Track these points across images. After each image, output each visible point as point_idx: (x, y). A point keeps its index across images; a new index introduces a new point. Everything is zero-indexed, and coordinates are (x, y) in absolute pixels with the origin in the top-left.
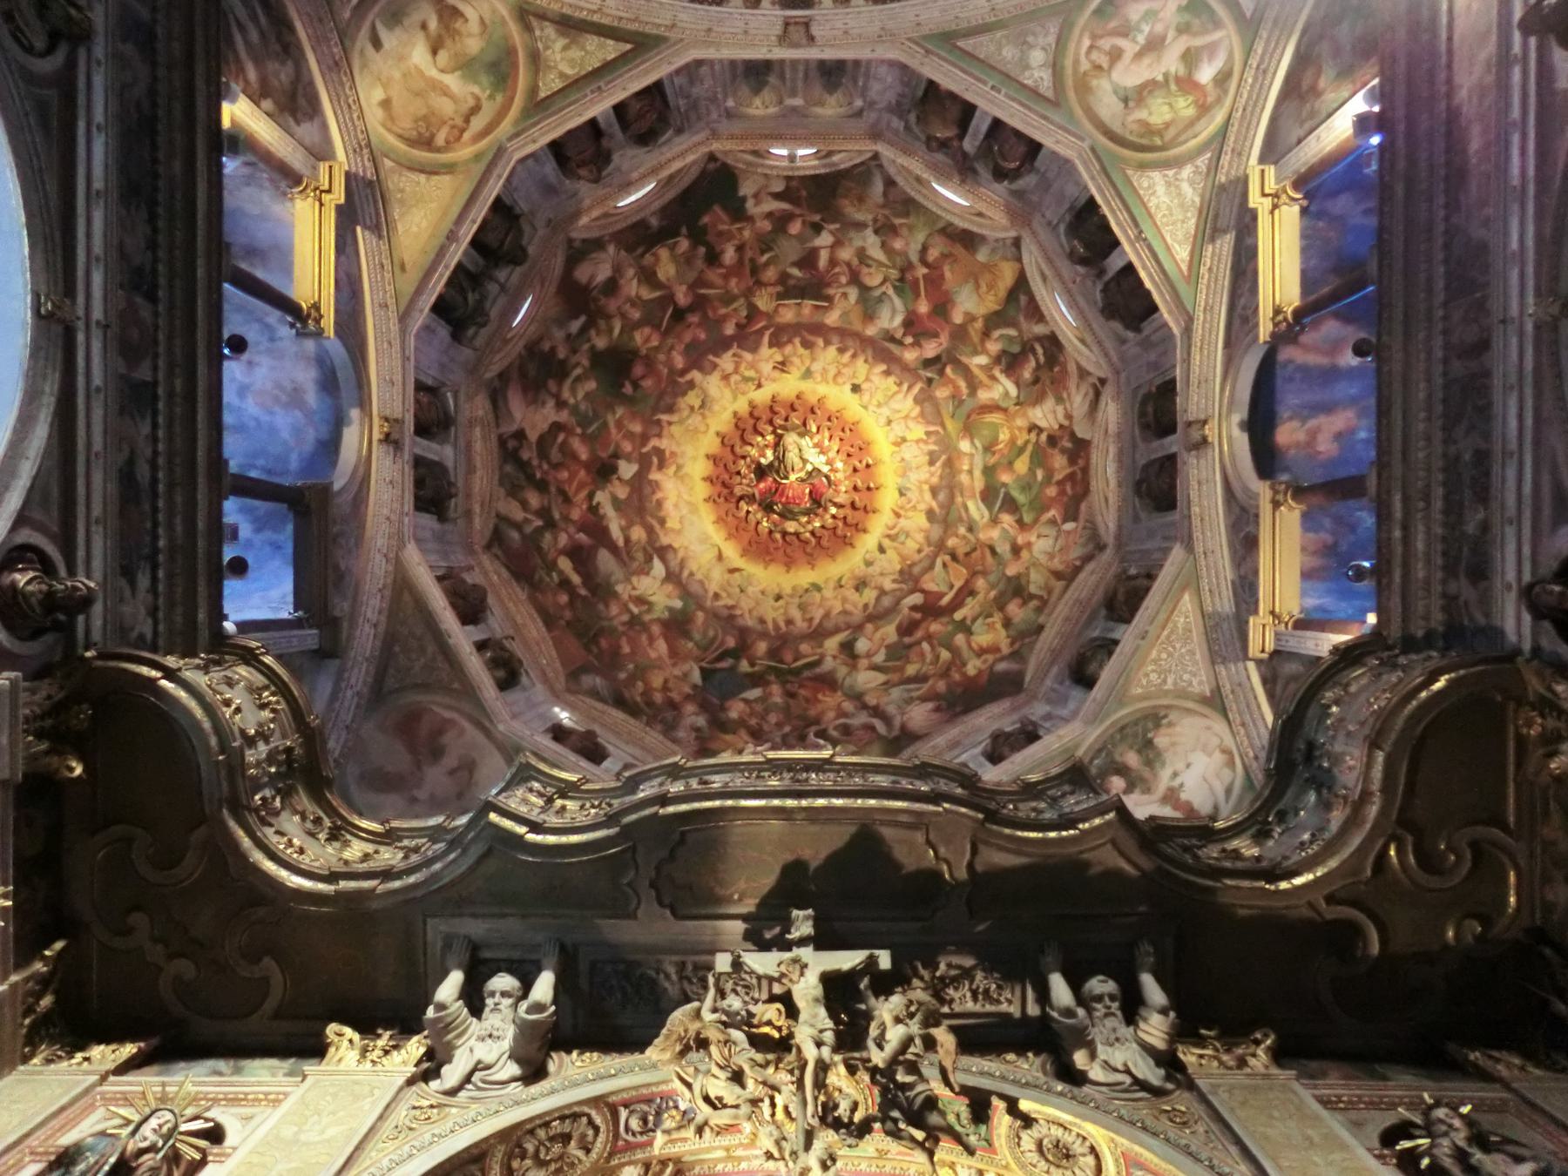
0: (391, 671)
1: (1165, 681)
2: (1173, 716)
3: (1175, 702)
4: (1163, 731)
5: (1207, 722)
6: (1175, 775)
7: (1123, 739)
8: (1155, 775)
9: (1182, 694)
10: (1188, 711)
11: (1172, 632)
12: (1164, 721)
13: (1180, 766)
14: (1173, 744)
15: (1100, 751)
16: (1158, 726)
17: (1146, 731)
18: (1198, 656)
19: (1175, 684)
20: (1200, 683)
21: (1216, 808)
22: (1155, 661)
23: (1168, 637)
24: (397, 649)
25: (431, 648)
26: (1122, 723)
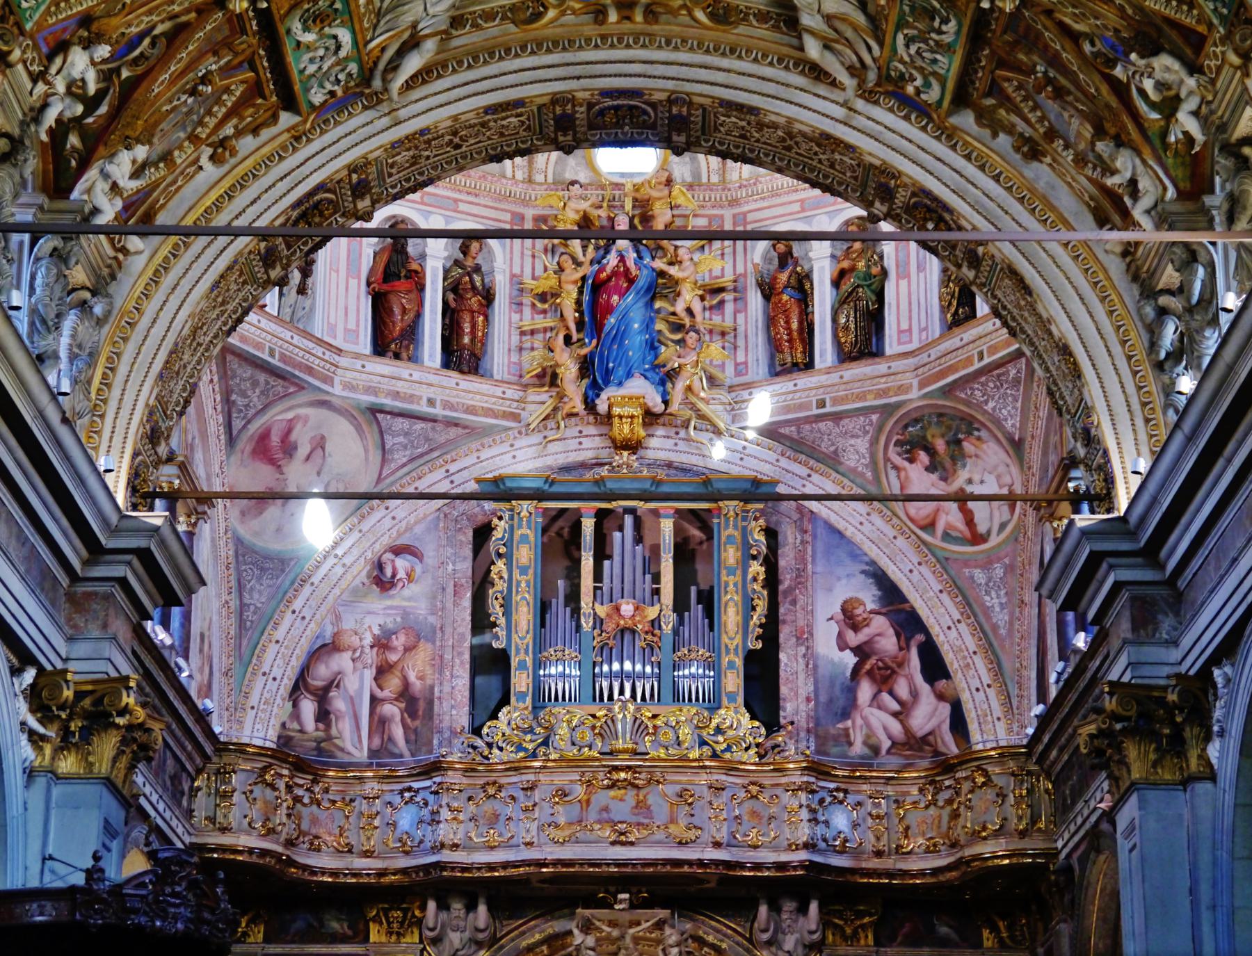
0: (235, 415)
1: (986, 402)
2: (984, 434)
3: (988, 424)
4: (972, 439)
5: (1009, 461)
6: (970, 481)
7: (939, 423)
8: (955, 471)
9: (998, 423)
10: (998, 440)
11: (1003, 374)
12: (976, 433)
13: (976, 478)
14: (977, 456)
15: (916, 421)
16: (969, 433)
17: (958, 431)
18: (1019, 405)
19: (994, 409)
20: (1013, 425)
21: (989, 532)
22: (983, 384)
23: (999, 376)
24: (234, 397)
25: (262, 377)
26: (942, 411)
